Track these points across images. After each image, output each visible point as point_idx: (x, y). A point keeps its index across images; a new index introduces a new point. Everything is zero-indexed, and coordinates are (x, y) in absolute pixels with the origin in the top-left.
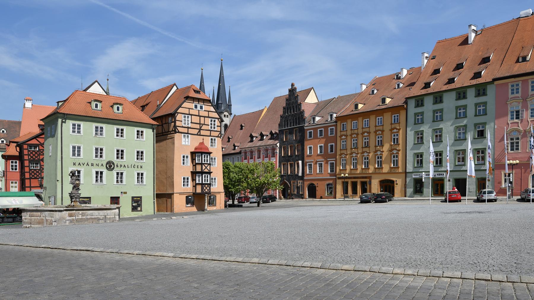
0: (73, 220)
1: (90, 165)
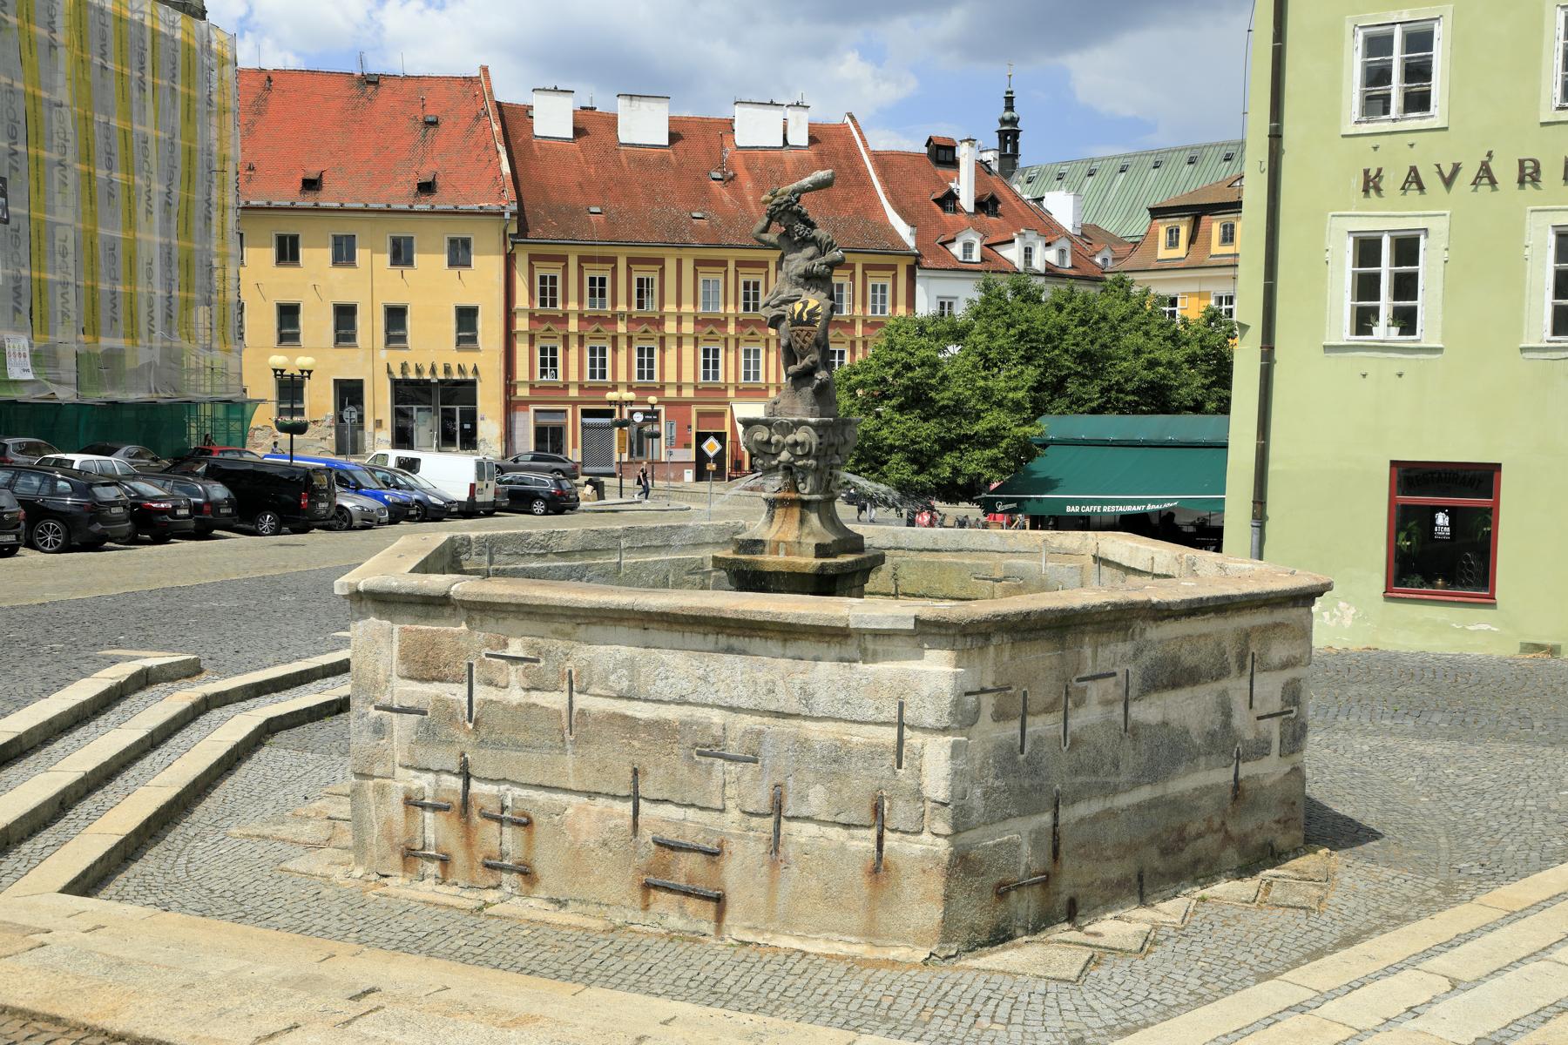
0: (446, 710)
1: (1505, 171)
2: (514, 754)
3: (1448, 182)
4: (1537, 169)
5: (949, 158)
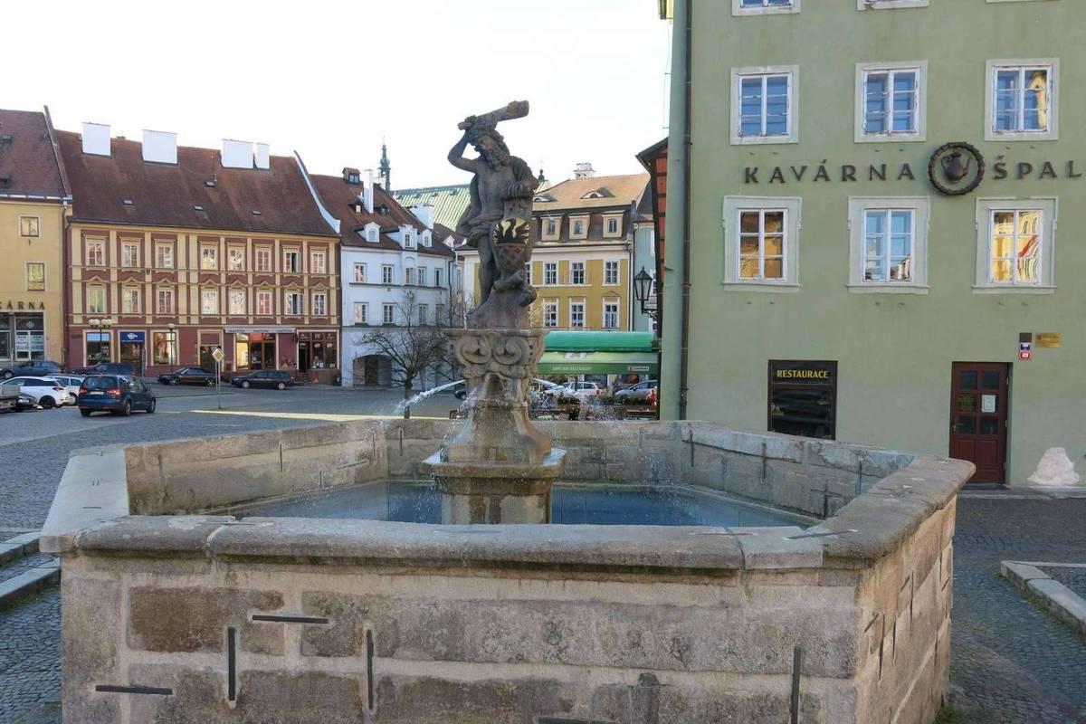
0: (200, 690)
3: (799, 177)
5: (356, 181)
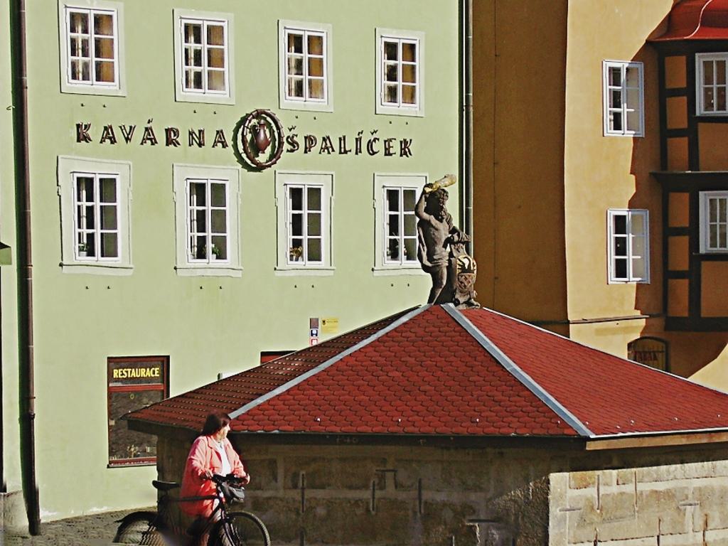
1: (161, 137)
2: (616, 524)
3: (127, 139)
4: (176, 133)
